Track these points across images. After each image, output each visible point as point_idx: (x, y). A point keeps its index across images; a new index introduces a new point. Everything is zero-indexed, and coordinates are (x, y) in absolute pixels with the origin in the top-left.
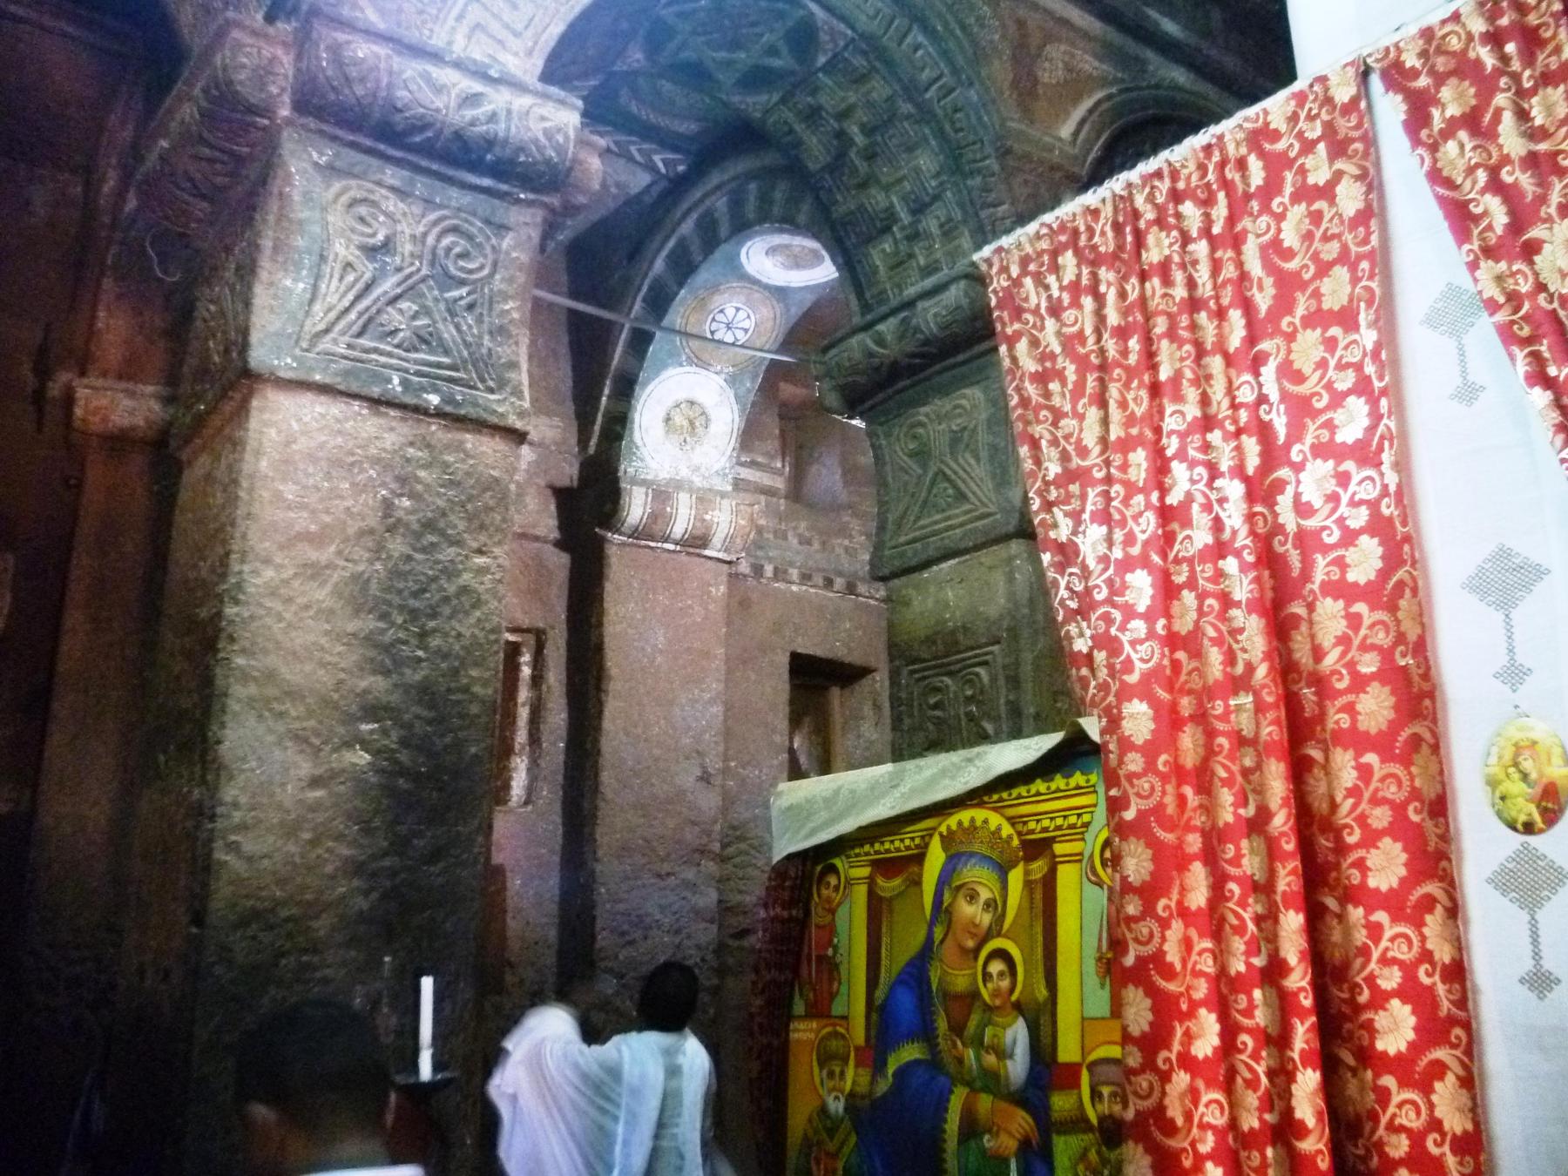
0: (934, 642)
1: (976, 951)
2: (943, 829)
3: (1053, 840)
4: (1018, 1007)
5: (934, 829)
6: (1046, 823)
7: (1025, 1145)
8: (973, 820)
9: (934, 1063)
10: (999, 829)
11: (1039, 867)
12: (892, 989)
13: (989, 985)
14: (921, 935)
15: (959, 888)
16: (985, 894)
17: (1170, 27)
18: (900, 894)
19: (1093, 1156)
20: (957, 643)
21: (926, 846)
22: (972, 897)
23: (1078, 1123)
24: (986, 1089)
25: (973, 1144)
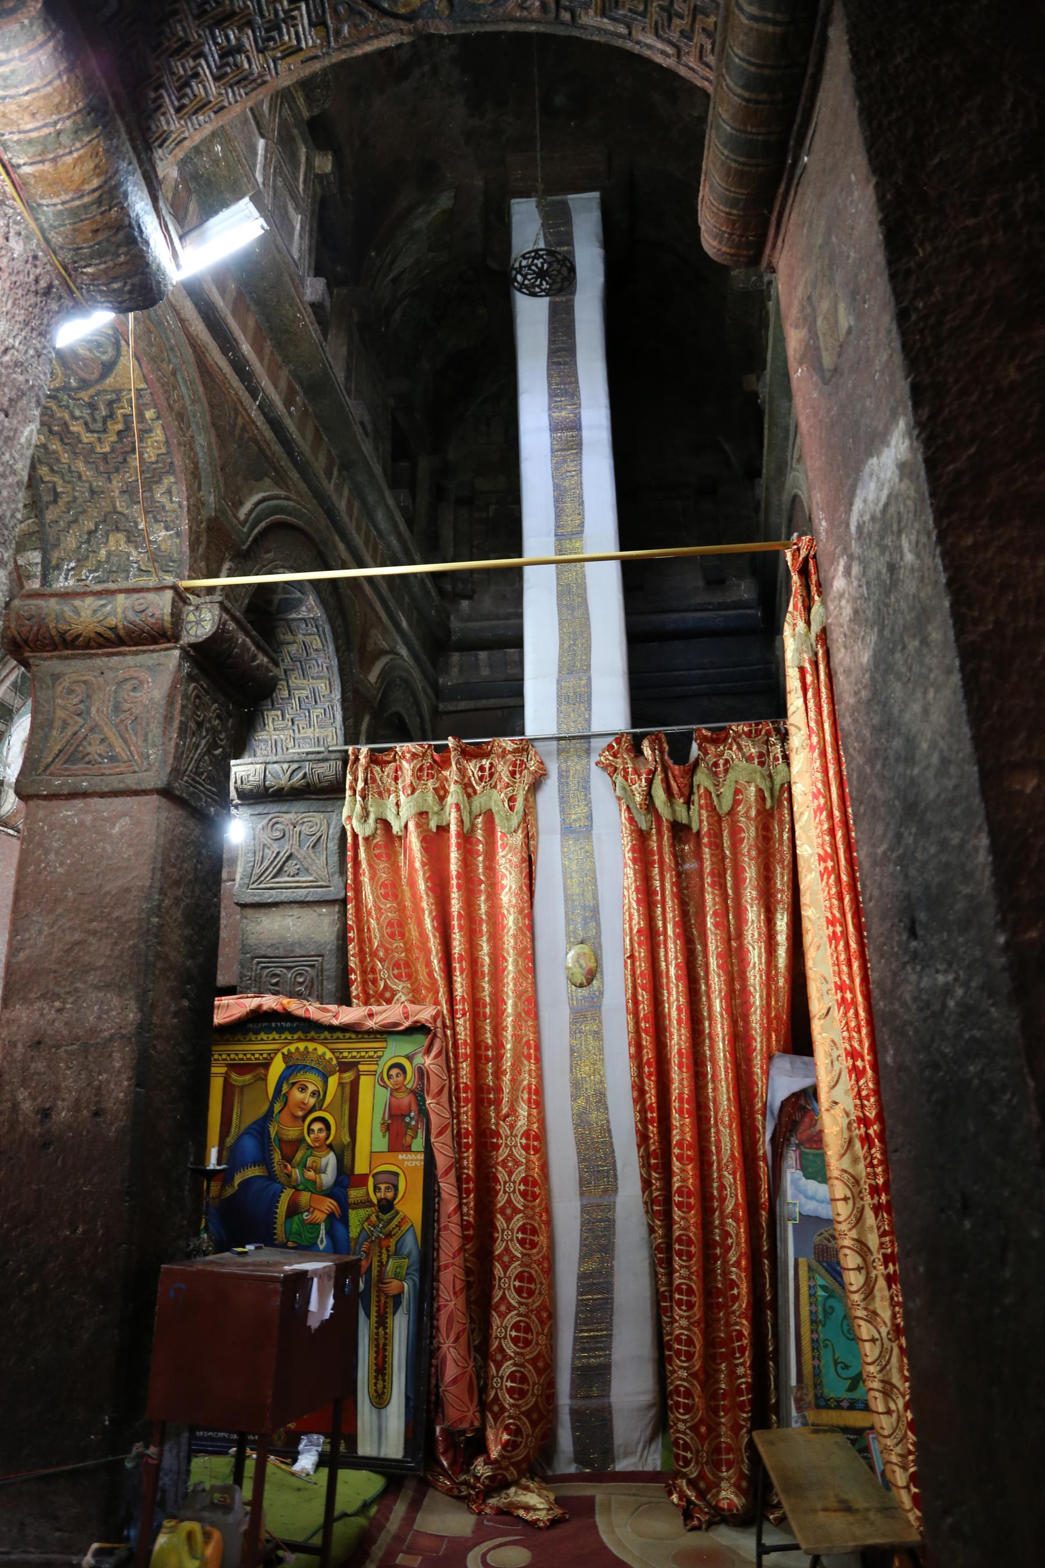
0: (278, 948)
1: (304, 1118)
2: (285, 1051)
3: (359, 1063)
4: (330, 1147)
5: (278, 1050)
6: (354, 1054)
7: (331, 1216)
8: (306, 1048)
9: (271, 1177)
10: (324, 1054)
11: (348, 1076)
12: (239, 1138)
13: (312, 1136)
14: (265, 1108)
15: (294, 1084)
16: (311, 1088)
17: (404, 624)
18: (250, 1084)
19: (373, 1218)
20: (293, 951)
21: (272, 1059)
22: (303, 1089)
23: (367, 1203)
24: (306, 1189)
25: (296, 1218)
